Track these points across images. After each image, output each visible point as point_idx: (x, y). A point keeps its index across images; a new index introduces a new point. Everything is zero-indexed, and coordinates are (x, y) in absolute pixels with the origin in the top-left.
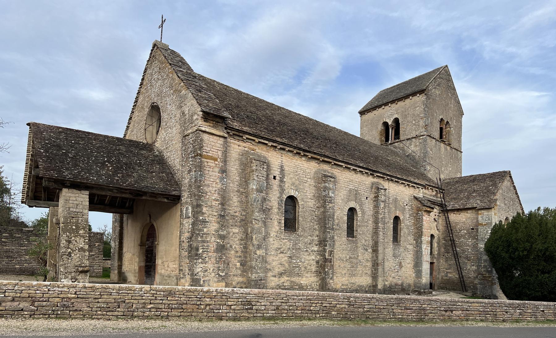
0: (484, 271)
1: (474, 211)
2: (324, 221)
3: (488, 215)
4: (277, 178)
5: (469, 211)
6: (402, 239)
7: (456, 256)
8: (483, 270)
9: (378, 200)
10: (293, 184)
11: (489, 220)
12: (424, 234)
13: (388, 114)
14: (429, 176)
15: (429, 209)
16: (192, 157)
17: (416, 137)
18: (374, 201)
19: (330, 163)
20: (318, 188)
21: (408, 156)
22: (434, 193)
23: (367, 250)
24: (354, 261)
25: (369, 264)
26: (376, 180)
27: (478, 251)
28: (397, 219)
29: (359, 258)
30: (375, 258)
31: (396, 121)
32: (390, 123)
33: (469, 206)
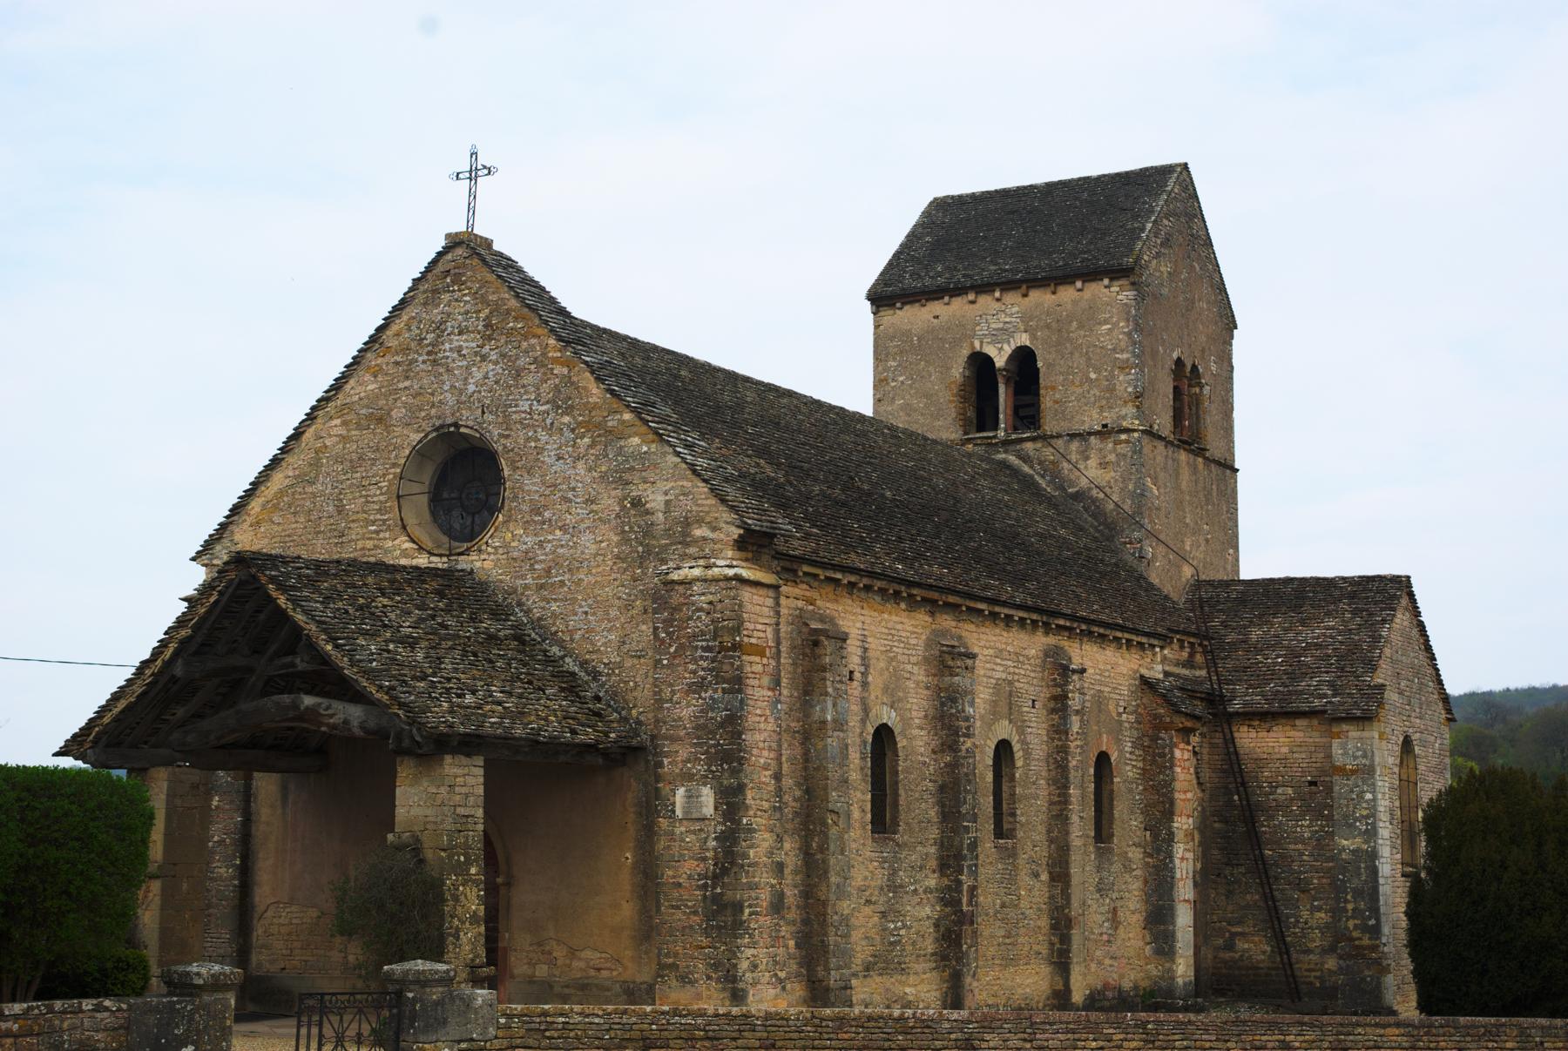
1: (1315, 722)
2: (951, 793)
4: (857, 675)
5: (1298, 722)
6: (1117, 831)
10: (886, 689)
11: (1365, 756)
12: (1177, 811)
13: (998, 325)
14: (1155, 581)
15: (1189, 724)
16: (705, 649)
17: (1105, 432)
22: (1185, 654)
23: (1036, 875)
24: (1012, 914)
25: (1044, 922)
26: (1051, 640)
28: (1103, 760)
29: (1023, 904)
32: (1000, 362)
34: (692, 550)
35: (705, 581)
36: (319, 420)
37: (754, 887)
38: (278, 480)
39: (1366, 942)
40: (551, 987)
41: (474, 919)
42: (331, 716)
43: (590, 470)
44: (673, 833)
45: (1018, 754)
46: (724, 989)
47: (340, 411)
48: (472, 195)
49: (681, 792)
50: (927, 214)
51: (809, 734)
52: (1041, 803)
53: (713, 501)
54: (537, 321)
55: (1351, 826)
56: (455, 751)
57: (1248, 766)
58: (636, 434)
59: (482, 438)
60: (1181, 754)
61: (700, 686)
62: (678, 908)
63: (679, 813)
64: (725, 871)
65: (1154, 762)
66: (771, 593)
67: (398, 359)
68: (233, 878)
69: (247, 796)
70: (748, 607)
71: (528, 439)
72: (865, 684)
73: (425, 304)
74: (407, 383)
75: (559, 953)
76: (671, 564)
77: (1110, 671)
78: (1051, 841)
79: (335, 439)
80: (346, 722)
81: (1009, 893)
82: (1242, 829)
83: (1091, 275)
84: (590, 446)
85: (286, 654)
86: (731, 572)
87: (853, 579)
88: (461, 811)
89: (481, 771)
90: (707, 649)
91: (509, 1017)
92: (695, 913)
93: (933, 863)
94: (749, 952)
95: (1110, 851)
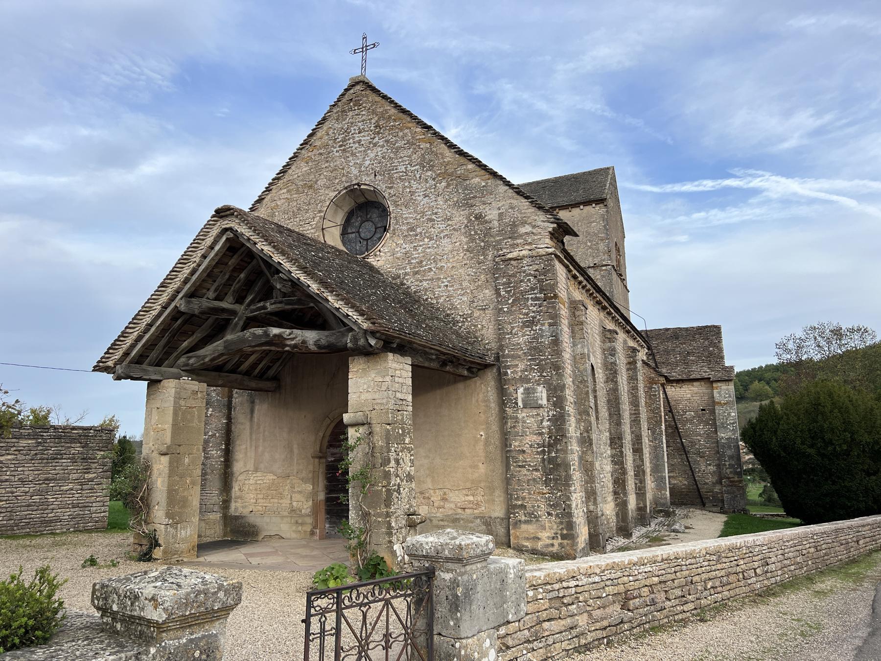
0: (731, 472)
1: (703, 383)
3: (727, 389)
34: (519, 241)
35: (532, 257)
36: (273, 191)
39: (736, 479)
40: (431, 521)
42: (293, 339)
43: (446, 201)
44: (517, 418)
46: (561, 523)
47: (286, 185)
48: (364, 60)
49: (521, 390)
53: (532, 210)
54: (409, 119)
56: (393, 351)
57: (672, 403)
58: (477, 176)
59: (375, 192)
61: (531, 323)
62: (523, 467)
63: (520, 404)
64: (557, 441)
65: (650, 398)
67: (322, 151)
68: (220, 457)
69: (229, 407)
73: (337, 120)
74: (326, 165)
75: (436, 498)
76: (505, 250)
79: (283, 201)
80: (304, 342)
84: (447, 187)
85: (259, 301)
88: (399, 395)
89: (410, 368)
90: (537, 299)
92: (537, 470)
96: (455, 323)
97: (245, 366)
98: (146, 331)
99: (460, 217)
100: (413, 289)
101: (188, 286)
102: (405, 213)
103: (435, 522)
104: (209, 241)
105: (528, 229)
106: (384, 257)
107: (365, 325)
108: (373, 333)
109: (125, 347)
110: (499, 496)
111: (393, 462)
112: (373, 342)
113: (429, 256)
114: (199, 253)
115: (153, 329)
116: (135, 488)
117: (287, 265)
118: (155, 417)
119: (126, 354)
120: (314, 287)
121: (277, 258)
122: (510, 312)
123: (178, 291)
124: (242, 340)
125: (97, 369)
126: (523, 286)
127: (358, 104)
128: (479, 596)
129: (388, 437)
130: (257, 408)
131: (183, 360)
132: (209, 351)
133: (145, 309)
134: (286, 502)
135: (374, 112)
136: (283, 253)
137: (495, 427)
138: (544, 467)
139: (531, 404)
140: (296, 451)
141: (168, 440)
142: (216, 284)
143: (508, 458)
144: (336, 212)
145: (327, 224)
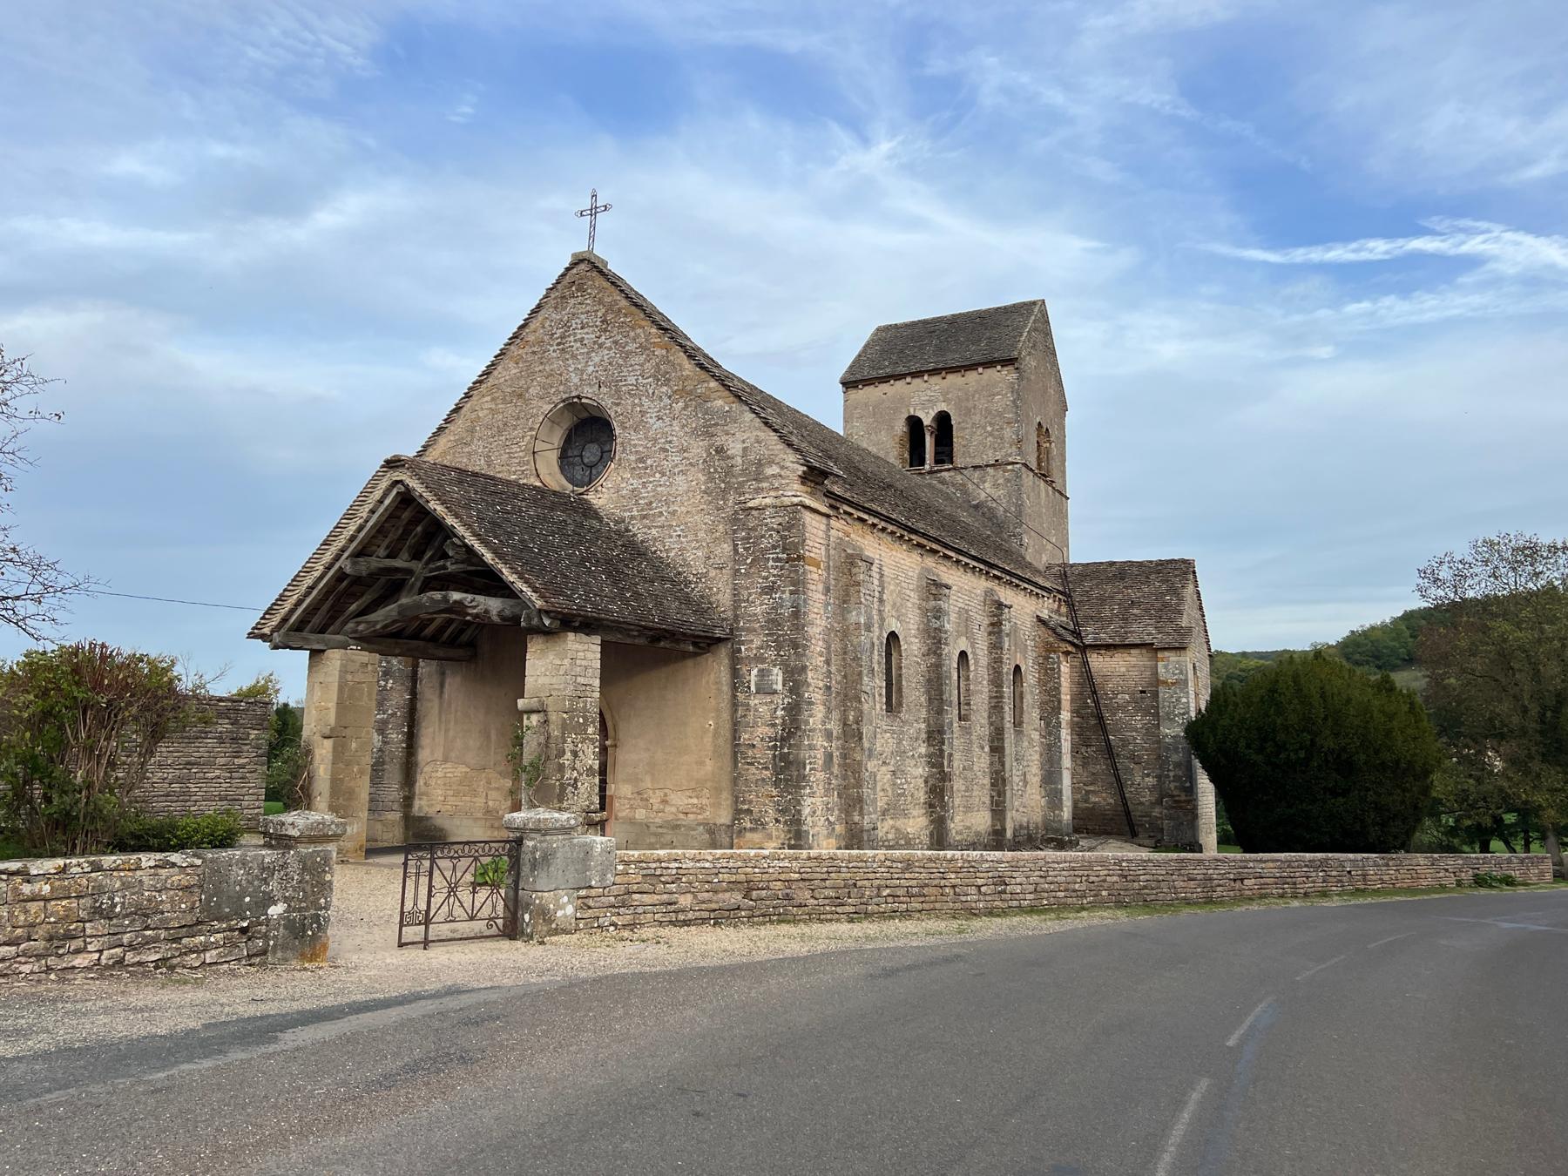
2: (935, 684)
7: (1110, 752)
8: (1172, 786)
9: (1001, 631)
13: (925, 398)
14: (1028, 559)
17: (997, 465)
18: (990, 634)
19: (935, 552)
20: (924, 612)
21: (976, 507)
24: (969, 774)
25: (987, 781)
27: (1159, 742)
28: (1017, 668)
30: (997, 767)
31: (943, 420)
32: (927, 421)
33: (1131, 640)
34: (765, 485)
37: (811, 747)
38: (443, 442)
41: (590, 770)
43: (683, 426)
45: (971, 662)
48: (593, 226)
49: (754, 672)
50: (875, 334)
51: (843, 632)
52: (985, 696)
53: (781, 446)
55: (1172, 720)
56: (576, 630)
59: (599, 408)
60: (1065, 668)
61: (770, 590)
63: (753, 688)
64: (791, 734)
66: (824, 520)
69: (414, 678)
70: (809, 528)
71: (634, 405)
72: (881, 601)
75: (655, 800)
77: (1024, 609)
78: (991, 724)
80: (486, 611)
81: (969, 760)
82: (1093, 722)
83: (989, 364)
86: (796, 500)
87: (876, 521)
88: (581, 680)
90: (777, 560)
91: (627, 863)
92: (767, 768)
93: (924, 736)
94: (809, 800)
95: (1021, 732)
96: (687, 583)
97: (428, 631)
98: (307, 594)
99: (698, 448)
100: (640, 537)
101: (354, 544)
102: (635, 438)
103: (653, 829)
104: (378, 494)
105: (774, 470)
106: (605, 496)
107: (539, 603)
108: (547, 612)
109: (283, 612)
110: (726, 798)
111: (568, 755)
112: (547, 622)
113: (659, 495)
114: (367, 508)
115: (315, 592)
116: (295, 776)
117: (461, 530)
118: (318, 693)
119: (284, 620)
120: (488, 557)
121: (450, 521)
122: (747, 575)
123: (343, 550)
124: (419, 606)
125: (251, 635)
126: (764, 543)
127: (581, 289)
128: (559, 861)
129: (564, 726)
130: (448, 681)
131: (351, 625)
132: (384, 615)
133: (306, 570)
134: (480, 801)
135: (601, 302)
136: (457, 516)
137: (726, 716)
138: (775, 764)
139: (765, 689)
140: (493, 737)
141: (332, 720)
142: (387, 541)
143: (735, 753)
144: (551, 430)
145: (539, 446)
